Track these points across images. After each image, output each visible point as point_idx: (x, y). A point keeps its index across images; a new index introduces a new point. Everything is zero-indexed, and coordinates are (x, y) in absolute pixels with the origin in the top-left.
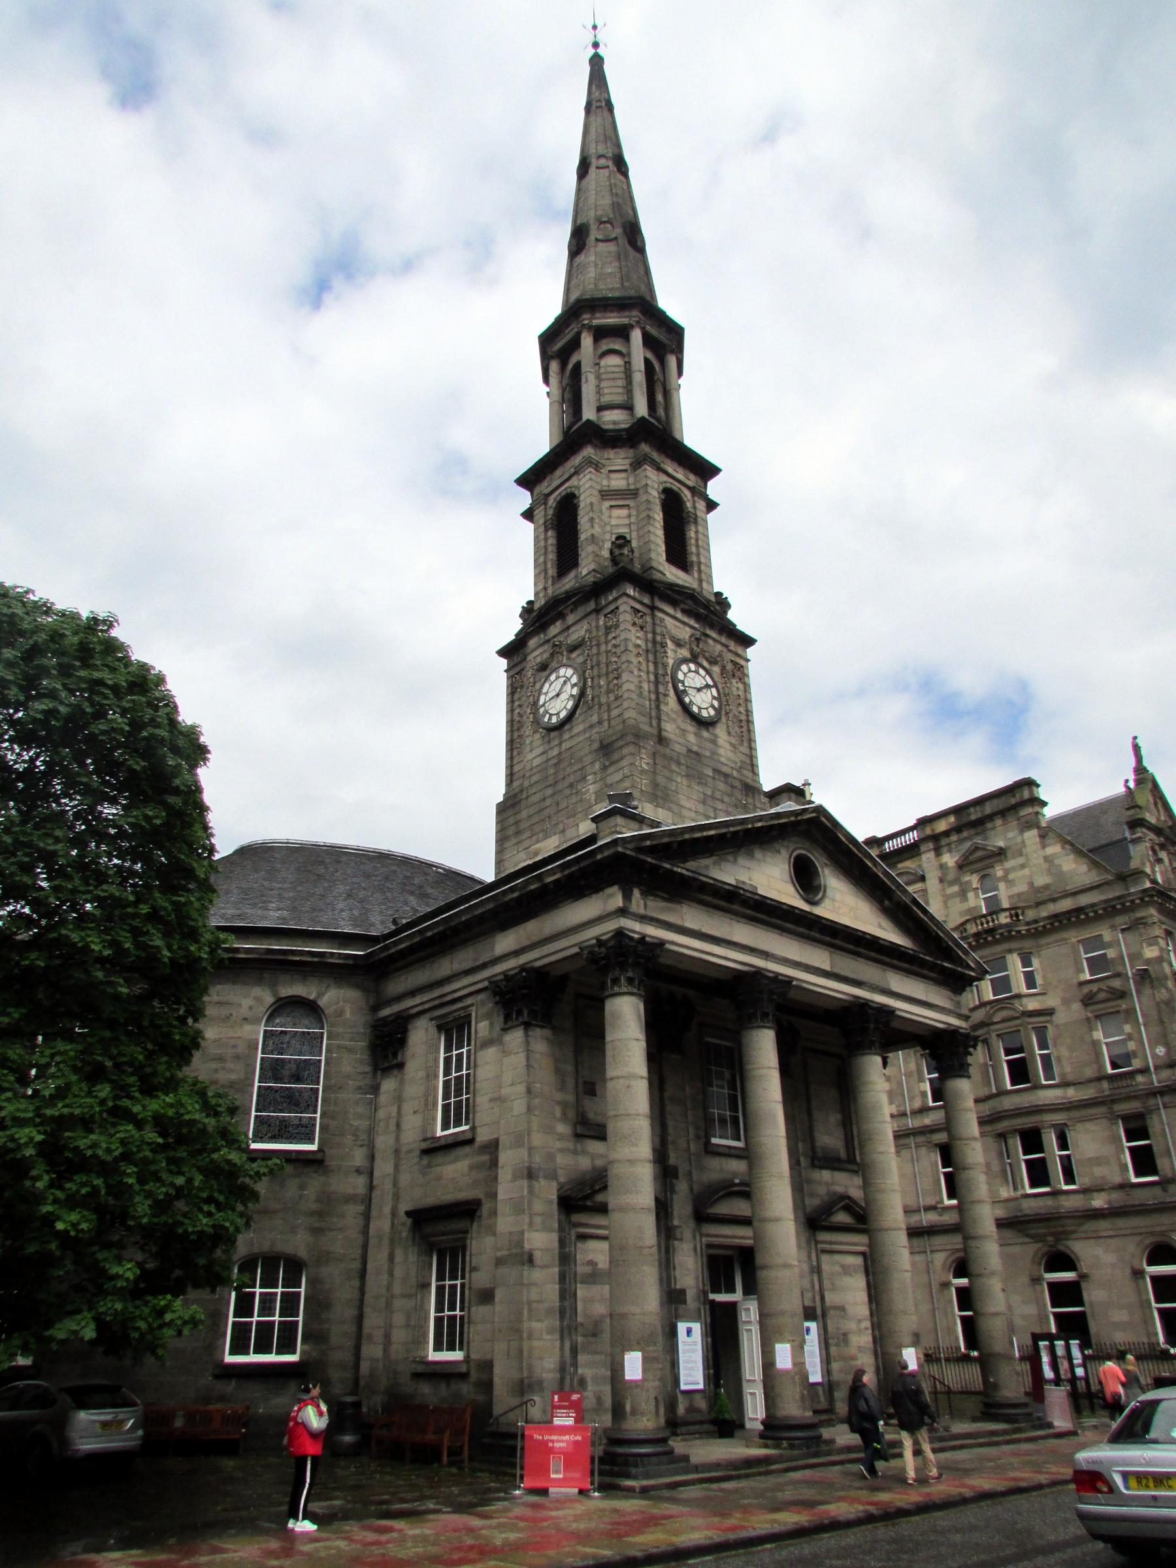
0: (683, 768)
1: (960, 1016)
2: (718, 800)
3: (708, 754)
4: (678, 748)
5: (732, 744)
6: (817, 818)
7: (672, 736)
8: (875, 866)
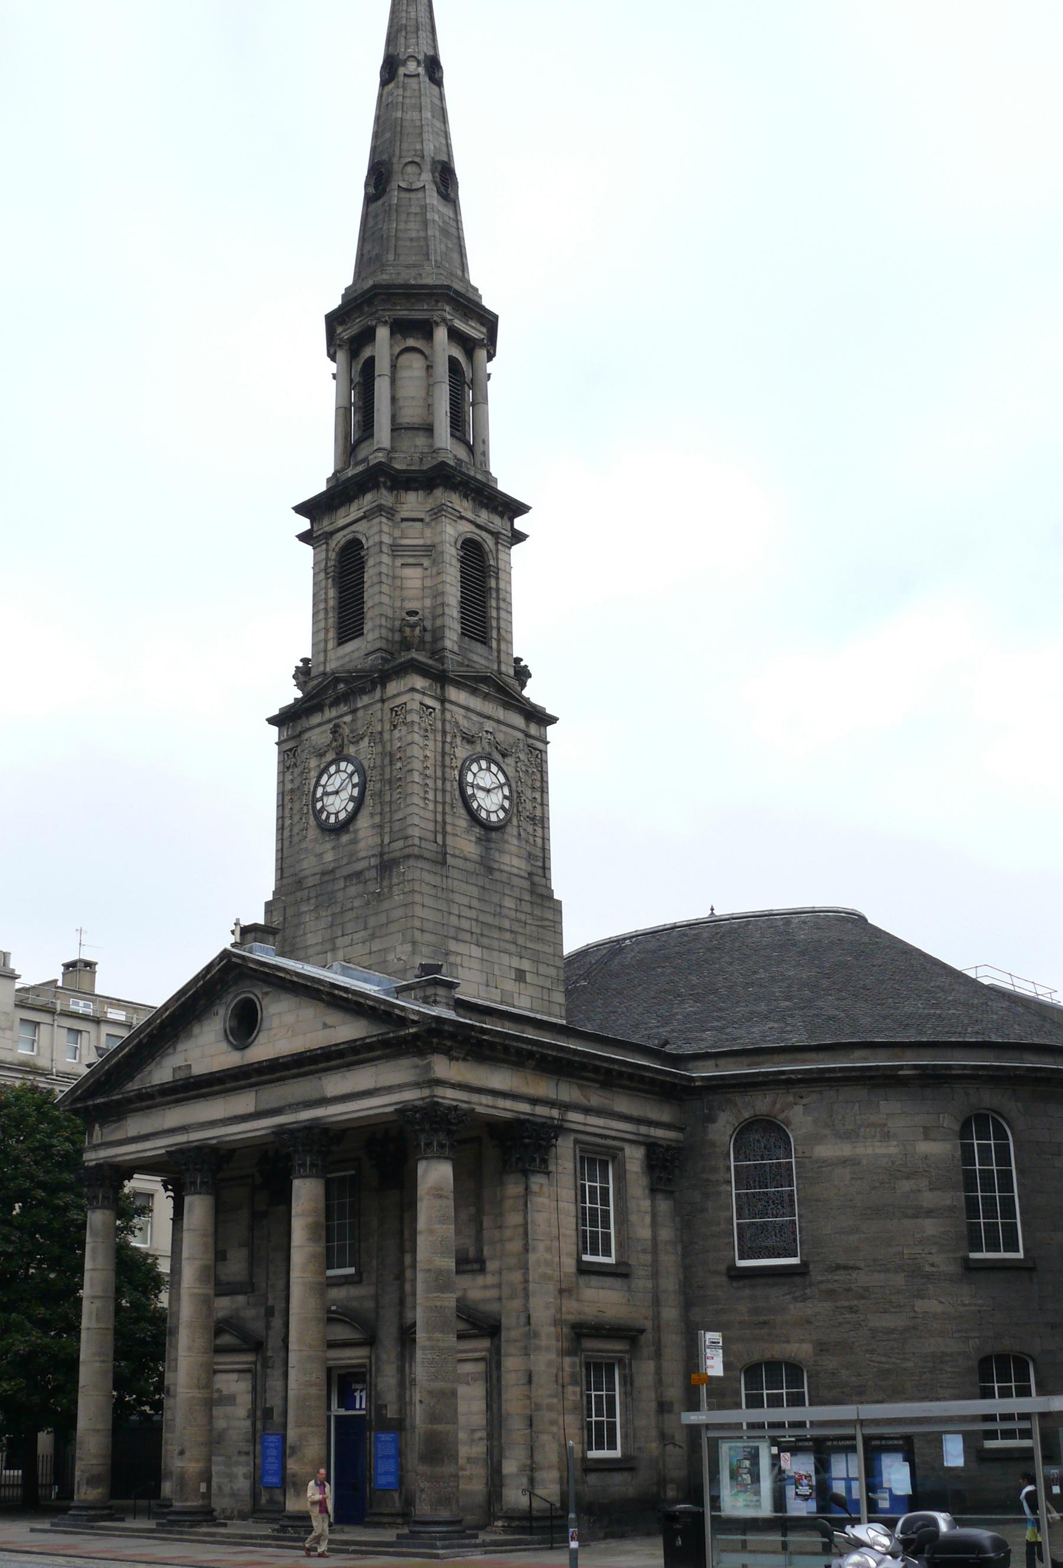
1: (417, 1085)
2: (349, 910)
3: (345, 861)
4: (310, 882)
5: (373, 826)
6: (229, 961)
7: (307, 873)
8: (288, 973)
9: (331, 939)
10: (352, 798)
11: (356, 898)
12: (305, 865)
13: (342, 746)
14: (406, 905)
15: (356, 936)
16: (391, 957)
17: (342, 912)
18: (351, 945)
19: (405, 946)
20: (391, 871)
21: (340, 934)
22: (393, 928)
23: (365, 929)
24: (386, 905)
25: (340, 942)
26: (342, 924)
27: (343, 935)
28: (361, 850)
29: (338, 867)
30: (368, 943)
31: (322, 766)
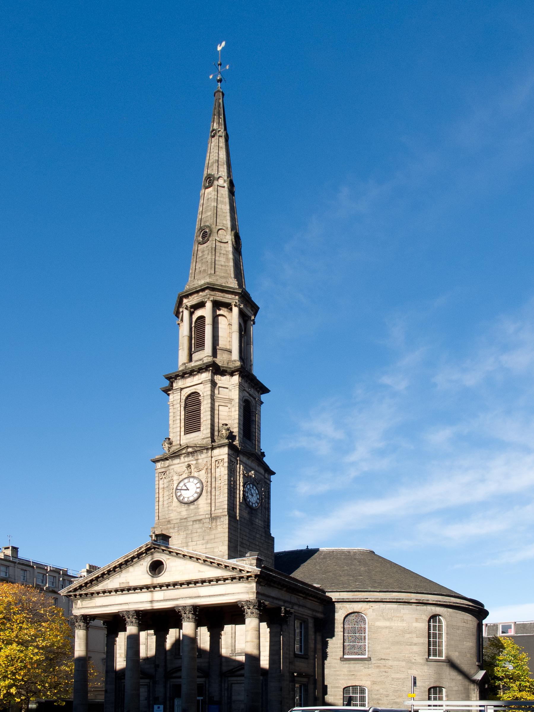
0: (177, 528)
3: (192, 516)
4: (175, 522)
7: (172, 518)
9: (186, 542)
10: (196, 492)
11: (198, 529)
12: (172, 515)
13: (191, 472)
14: (224, 533)
15: (198, 542)
16: (216, 550)
17: (192, 533)
18: (196, 545)
19: (223, 547)
20: (216, 520)
21: (190, 541)
22: (216, 540)
23: (203, 540)
24: (214, 532)
25: (190, 544)
26: (192, 538)
27: (192, 541)
28: (200, 512)
29: (189, 517)
30: (205, 545)
31: (180, 480)
